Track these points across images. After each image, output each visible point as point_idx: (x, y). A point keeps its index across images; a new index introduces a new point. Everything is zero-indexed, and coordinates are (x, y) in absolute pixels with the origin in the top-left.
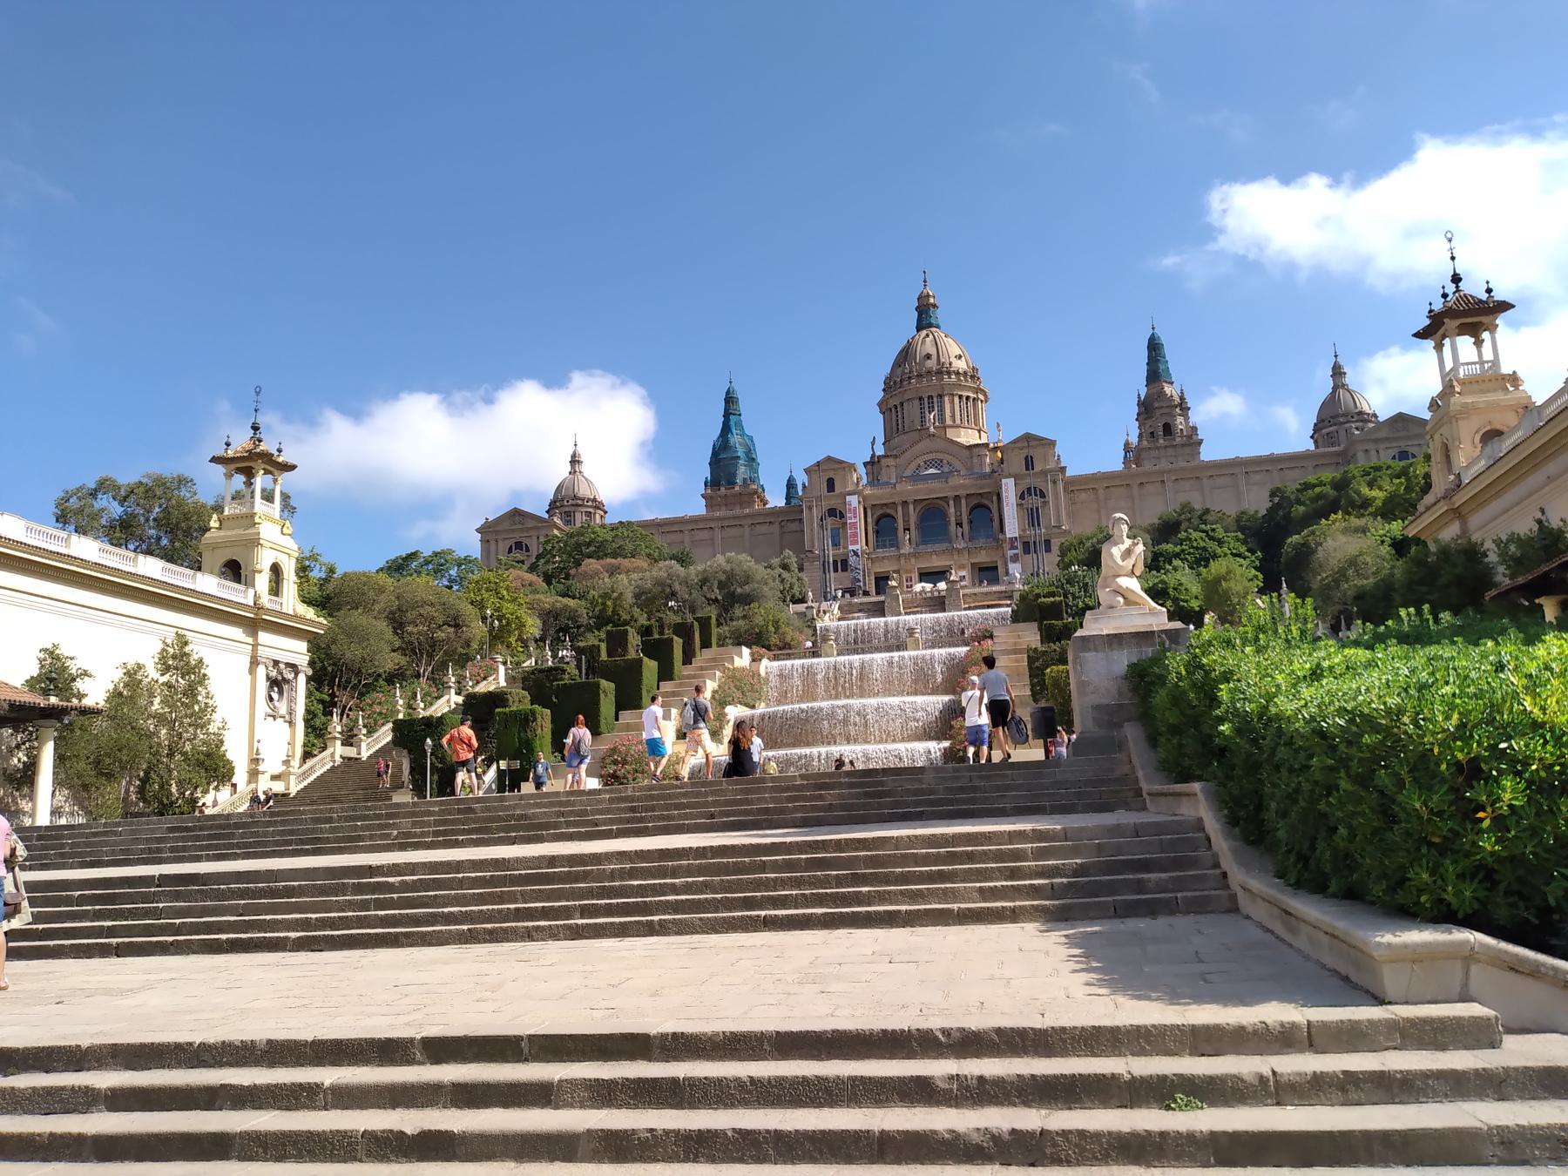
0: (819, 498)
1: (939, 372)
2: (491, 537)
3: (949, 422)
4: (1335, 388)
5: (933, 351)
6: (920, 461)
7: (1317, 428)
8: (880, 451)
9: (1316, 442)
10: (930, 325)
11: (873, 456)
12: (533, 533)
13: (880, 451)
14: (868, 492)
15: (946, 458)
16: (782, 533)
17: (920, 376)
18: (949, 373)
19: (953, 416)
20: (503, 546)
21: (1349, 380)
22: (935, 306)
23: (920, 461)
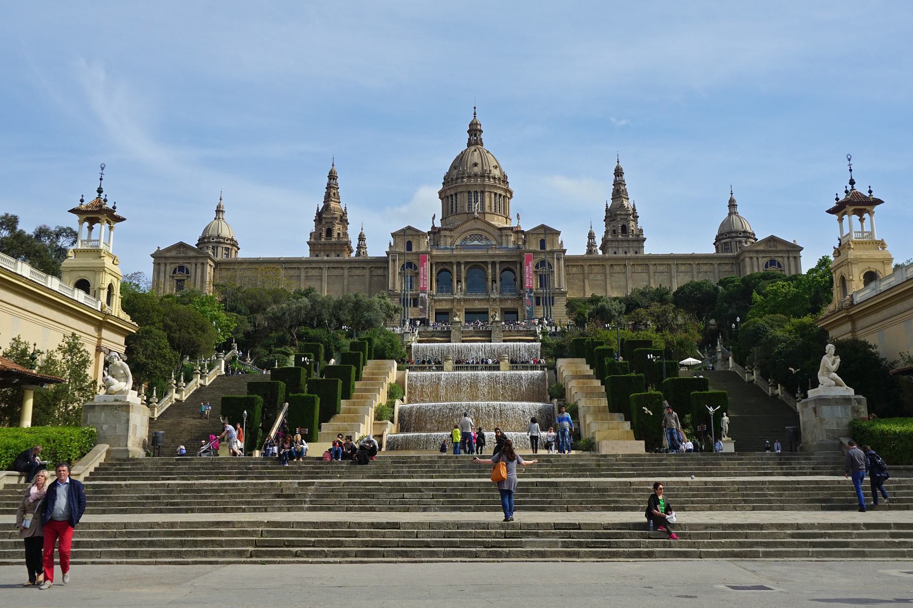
0: (400, 254)
1: (483, 176)
2: (162, 261)
3: (487, 210)
4: (730, 214)
5: (479, 161)
6: (467, 235)
7: (718, 239)
8: (438, 224)
9: (717, 247)
10: (477, 144)
11: (433, 227)
12: (193, 261)
13: (438, 224)
14: (435, 253)
15: (485, 234)
17: (469, 177)
18: (489, 177)
19: (490, 207)
20: (170, 269)
21: (738, 210)
22: (481, 131)
23: (467, 235)
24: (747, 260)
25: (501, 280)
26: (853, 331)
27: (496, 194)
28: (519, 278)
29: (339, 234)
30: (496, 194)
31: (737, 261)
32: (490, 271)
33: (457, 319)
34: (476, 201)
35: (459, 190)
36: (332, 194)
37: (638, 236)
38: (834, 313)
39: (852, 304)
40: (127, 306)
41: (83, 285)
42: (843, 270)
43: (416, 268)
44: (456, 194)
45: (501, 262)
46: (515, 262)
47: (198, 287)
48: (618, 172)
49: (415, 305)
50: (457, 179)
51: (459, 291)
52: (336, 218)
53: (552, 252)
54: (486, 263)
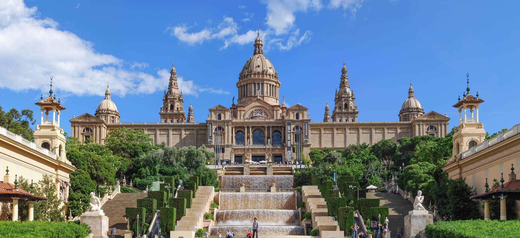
3: (265, 94)
6: (253, 110)
7: (401, 113)
9: (400, 117)
11: (233, 105)
16: (197, 134)
17: (255, 74)
23: (253, 110)
24: (417, 127)
25: (273, 137)
26: (460, 173)
27: (270, 85)
28: (283, 136)
29: (178, 108)
30: (270, 85)
31: (411, 127)
32: (266, 132)
33: (247, 161)
34: (258, 90)
35: (249, 82)
36: (173, 83)
37: (354, 110)
38: (452, 163)
39: (461, 159)
40: (70, 157)
41: (46, 145)
42: (458, 139)
43: (223, 130)
44: (247, 85)
45: (273, 127)
46: (281, 127)
47: (98, 142)
48: (344, 71)
49: (223, 151)
50: (247, 75)
51: (249, 144)
52: (176, 99)
53: (302, 121)
54: (264, 127)
